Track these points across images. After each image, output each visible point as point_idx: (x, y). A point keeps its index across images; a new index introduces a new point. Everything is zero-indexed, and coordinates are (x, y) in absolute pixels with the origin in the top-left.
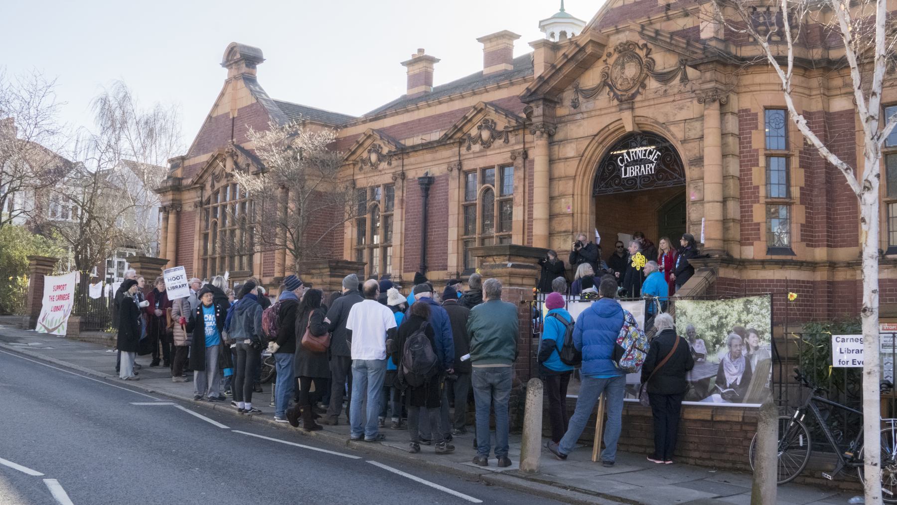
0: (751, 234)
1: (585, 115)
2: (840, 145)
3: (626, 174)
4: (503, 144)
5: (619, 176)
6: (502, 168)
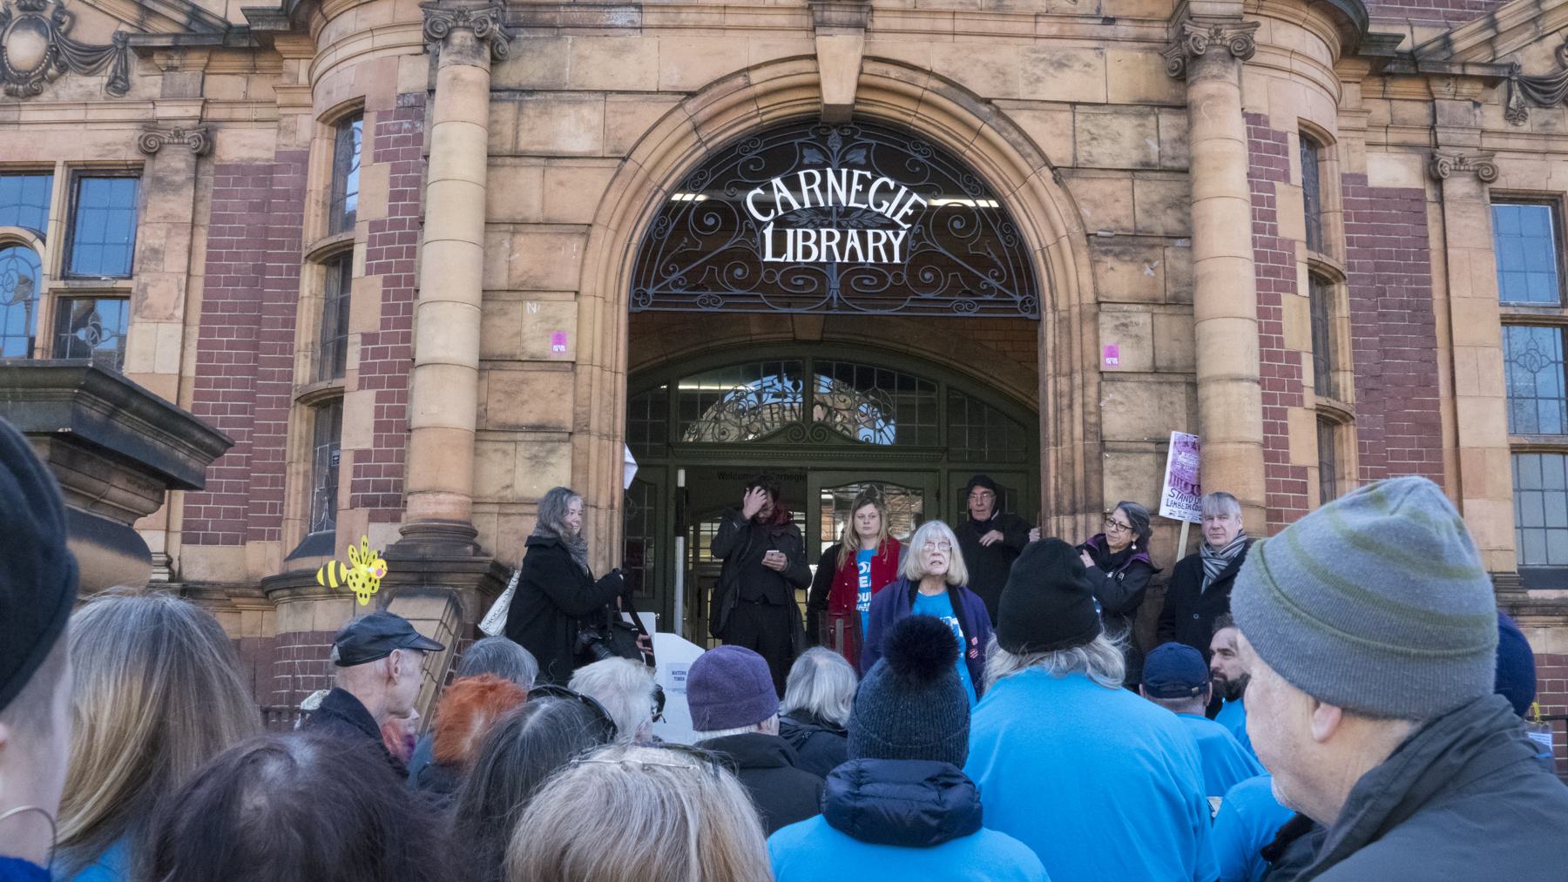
0: (1285, 502)
1: (651, 18)
2: (1390, 280)
3: (779, 249)
4: (100, 95)
5: (751, 255)
6: (81, 173)
